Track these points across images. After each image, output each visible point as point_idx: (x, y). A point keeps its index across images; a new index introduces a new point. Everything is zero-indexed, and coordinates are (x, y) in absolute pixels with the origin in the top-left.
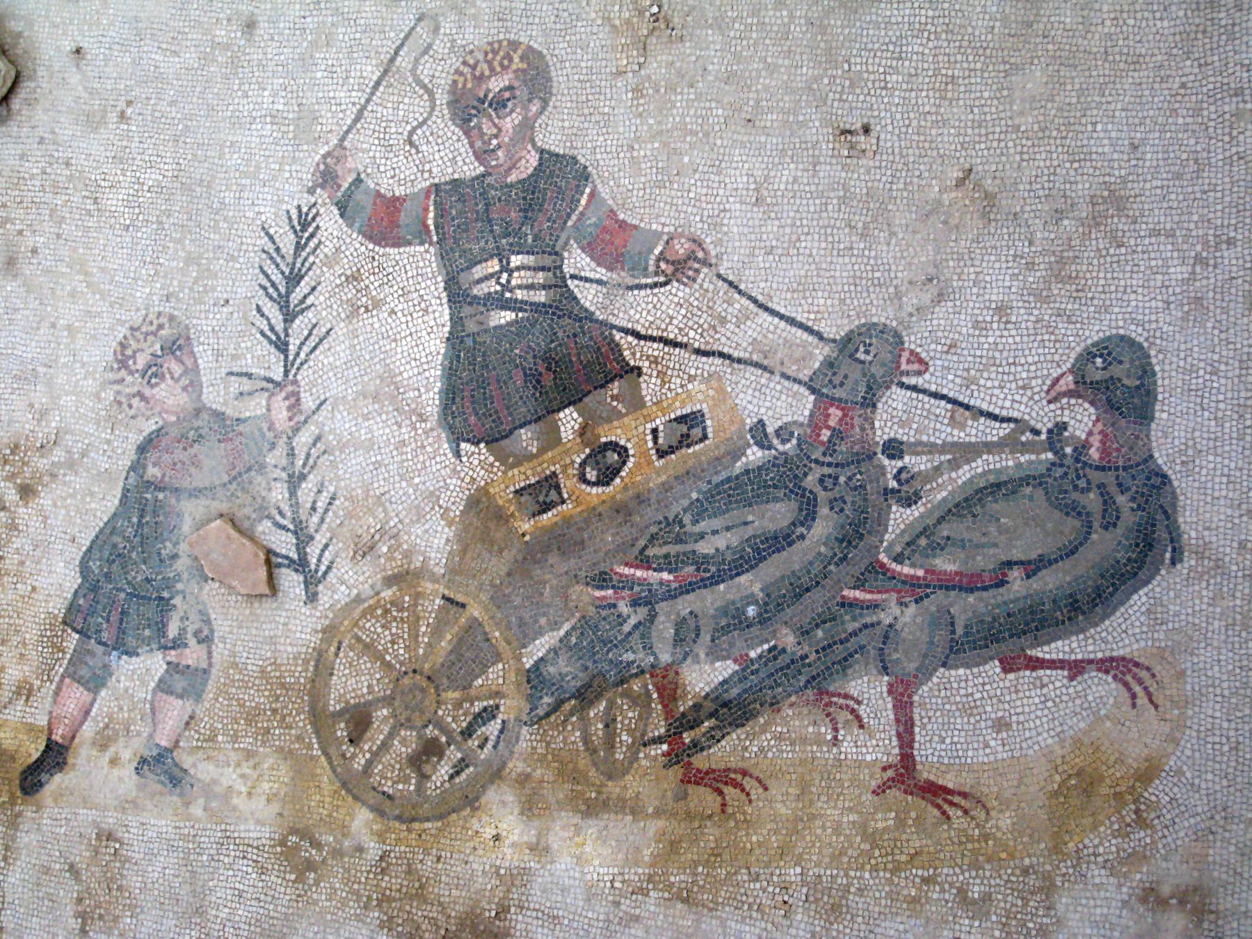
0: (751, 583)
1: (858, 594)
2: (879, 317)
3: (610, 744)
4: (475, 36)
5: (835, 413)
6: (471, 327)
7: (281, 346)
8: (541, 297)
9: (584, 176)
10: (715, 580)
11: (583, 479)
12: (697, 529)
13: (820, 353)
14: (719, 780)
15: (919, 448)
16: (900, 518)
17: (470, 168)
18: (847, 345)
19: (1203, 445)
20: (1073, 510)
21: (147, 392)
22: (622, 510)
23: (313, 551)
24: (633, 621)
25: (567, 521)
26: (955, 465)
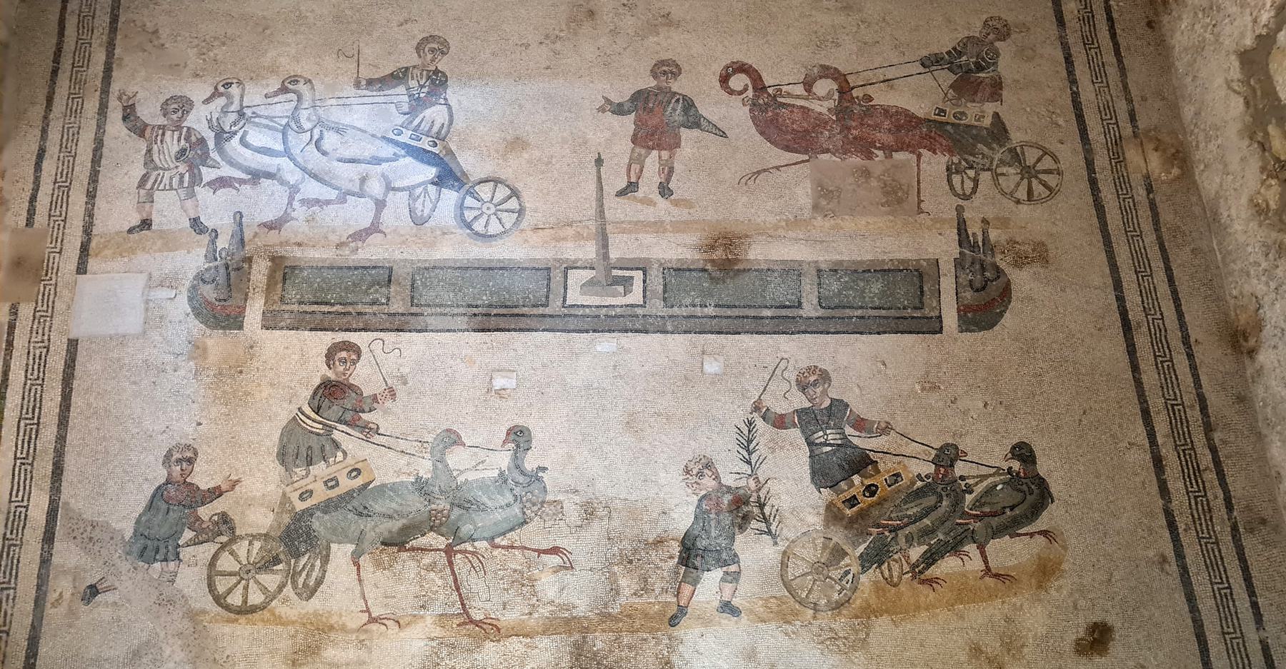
0: (927, 521)
1: (961, 521)
2: (950, 441)
3: (891, 576)
4: (804, 364)
5: (942, 470)
6: (817, 452)
7: (749, 463)
8: (839, 442)
9: (847, 406)
10: (915, 522)
11: (864, 495)
12: (906, 507)
13: (934, 452)
14: (930, 582)
15: (968, 477)
16: (969, 498)
17: (808, 405)
18: (941, 449)
19: (1052, 469)
20: (1019, 490)
21: (699, 481)
22: (879, 503)
23: (773, 528)
24: (891, 537)
25: (862, 509)
26: (981, 481)
